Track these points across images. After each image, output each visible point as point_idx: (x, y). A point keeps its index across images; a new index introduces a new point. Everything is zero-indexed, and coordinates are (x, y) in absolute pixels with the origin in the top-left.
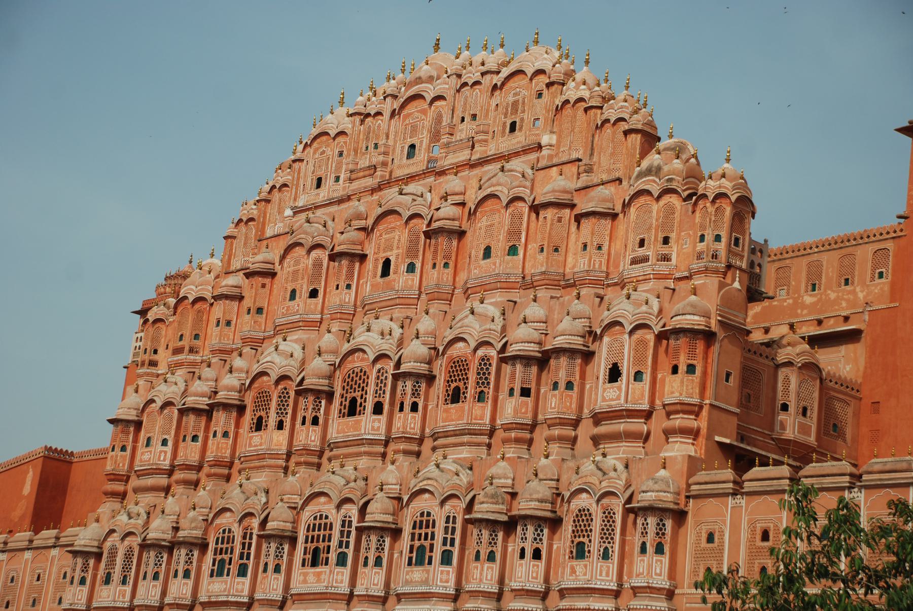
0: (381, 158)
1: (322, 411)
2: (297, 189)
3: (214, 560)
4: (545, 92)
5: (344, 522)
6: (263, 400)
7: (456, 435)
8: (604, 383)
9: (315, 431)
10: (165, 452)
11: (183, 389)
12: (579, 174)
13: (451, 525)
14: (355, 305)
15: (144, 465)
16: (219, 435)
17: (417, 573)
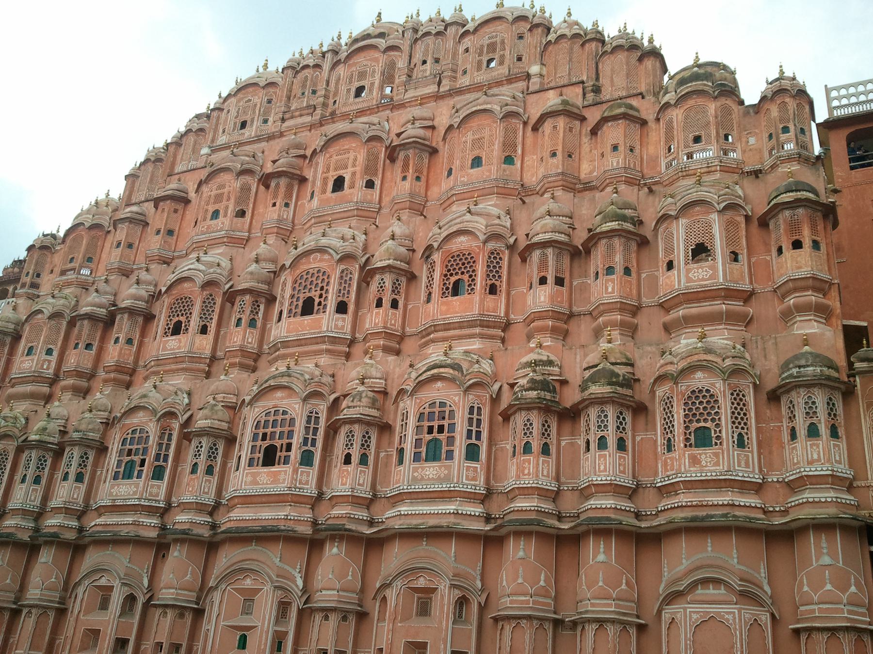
0: (321, 99)
1: (260, 315)
2: (215, 133)
3: (119, 462)
4: (527, 35)
5: (309, 417)
6: (184, 304)
7: (461, 328)
8: (686, 264)
9: (252, 333)
10: (50, 362)
11: (73, 303)
12: (584, 94)
13: (475, 416)
14: (293, 222)
15: (25, 373)
16: (122, 340)
17: (431, 470)
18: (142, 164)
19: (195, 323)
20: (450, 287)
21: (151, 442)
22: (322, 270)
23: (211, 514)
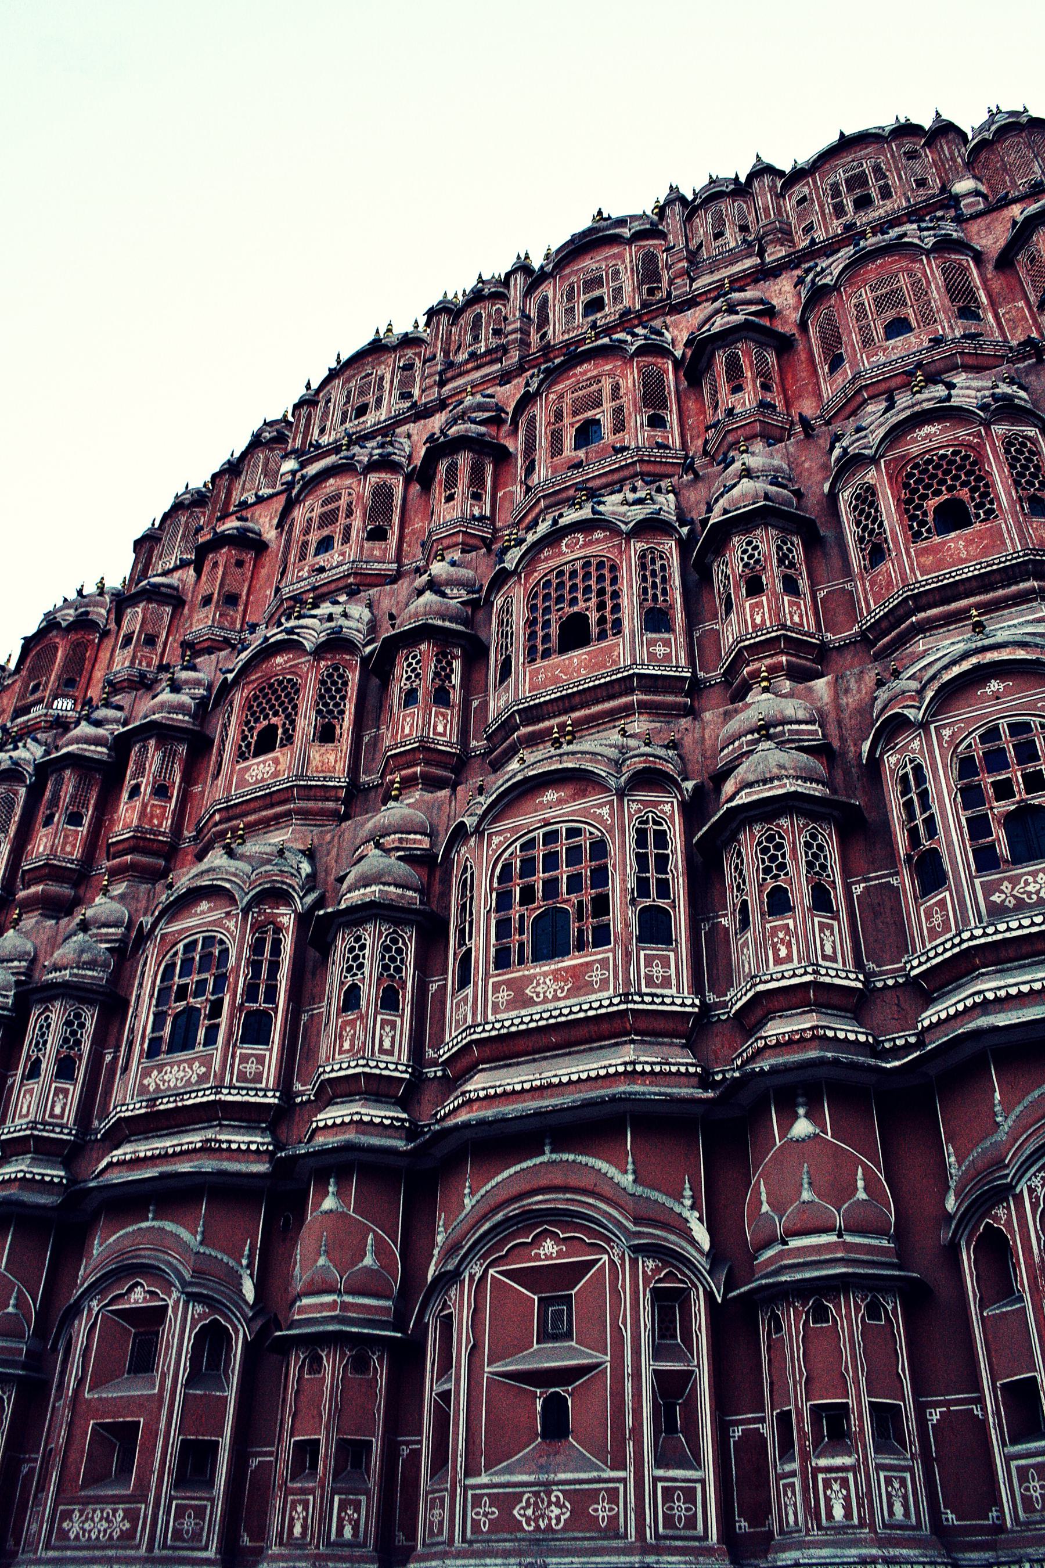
5: (641, 834)
9: (444, 716)
16: (146, 789)
18: (166, 516)
19: (306, 723)
20: (930, 519)
21: (232, 961)
22: (594, 562)
23: (403, 1103)
